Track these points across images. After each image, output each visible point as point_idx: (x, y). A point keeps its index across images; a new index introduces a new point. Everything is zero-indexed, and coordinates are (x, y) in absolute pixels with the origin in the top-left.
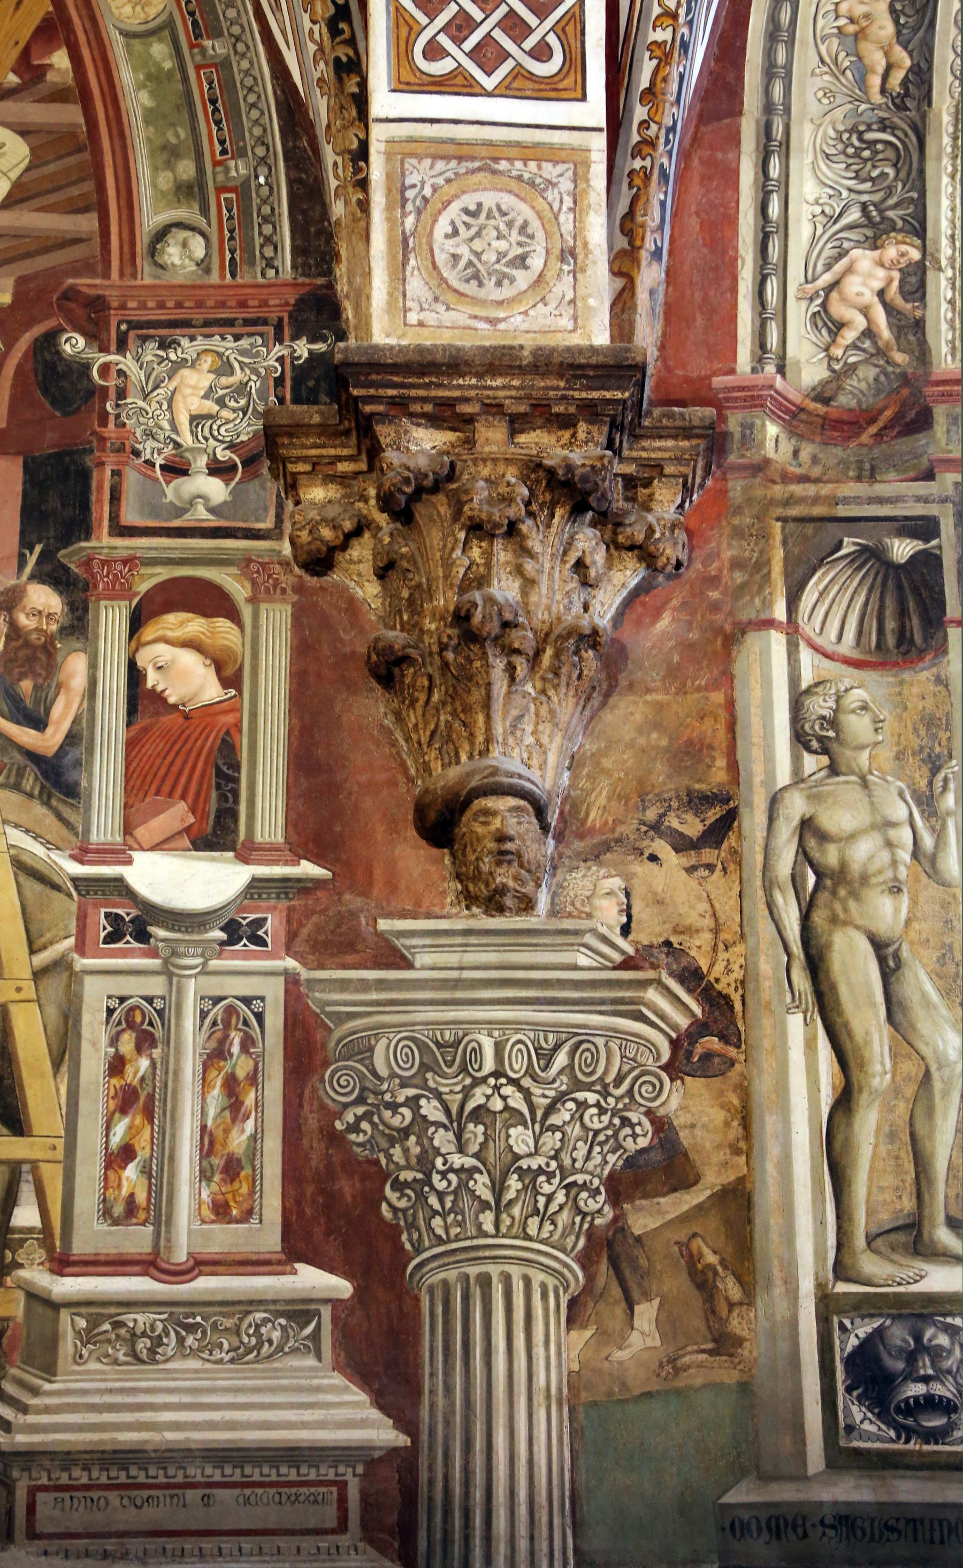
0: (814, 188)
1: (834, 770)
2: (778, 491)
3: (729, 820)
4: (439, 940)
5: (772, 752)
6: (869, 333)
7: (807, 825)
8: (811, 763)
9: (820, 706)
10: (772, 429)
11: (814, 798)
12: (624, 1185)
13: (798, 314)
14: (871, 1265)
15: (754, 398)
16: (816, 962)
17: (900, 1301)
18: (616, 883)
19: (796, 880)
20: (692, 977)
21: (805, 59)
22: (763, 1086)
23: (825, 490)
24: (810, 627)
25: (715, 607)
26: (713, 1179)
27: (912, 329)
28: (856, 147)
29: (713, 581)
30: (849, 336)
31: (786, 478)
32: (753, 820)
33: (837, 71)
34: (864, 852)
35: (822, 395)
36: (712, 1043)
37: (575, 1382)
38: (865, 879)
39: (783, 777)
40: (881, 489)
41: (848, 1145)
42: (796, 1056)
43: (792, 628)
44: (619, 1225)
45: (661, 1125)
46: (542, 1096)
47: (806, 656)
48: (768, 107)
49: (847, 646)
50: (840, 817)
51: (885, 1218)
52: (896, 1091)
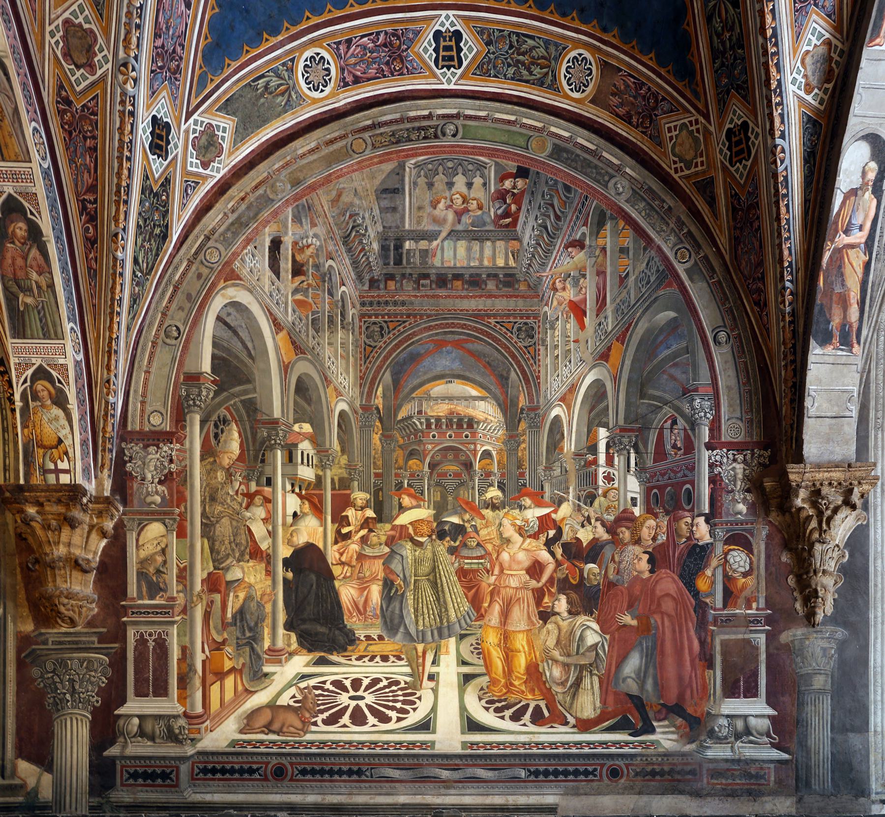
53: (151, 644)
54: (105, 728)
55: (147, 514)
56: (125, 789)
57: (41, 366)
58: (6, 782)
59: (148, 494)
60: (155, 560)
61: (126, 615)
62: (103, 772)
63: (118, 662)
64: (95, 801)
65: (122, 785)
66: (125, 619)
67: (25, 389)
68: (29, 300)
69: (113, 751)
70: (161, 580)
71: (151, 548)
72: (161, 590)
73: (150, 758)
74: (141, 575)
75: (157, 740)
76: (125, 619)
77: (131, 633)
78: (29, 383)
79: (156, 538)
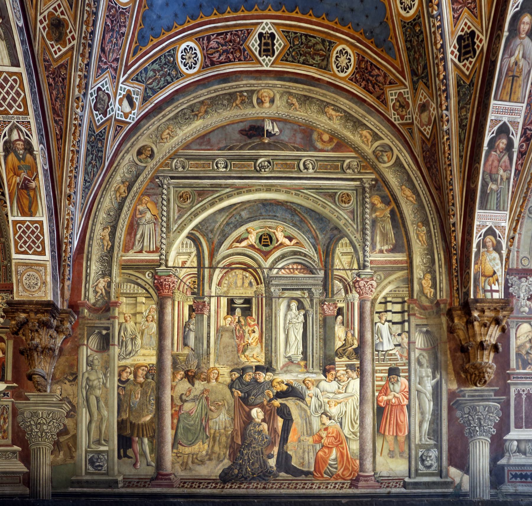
0: (95, 267)
1: (92, 369)
2: (86, 321)
3: (76, 378)
4: (33, 397)
5: (84, 367)
6: (102, 294)
7: (88, 379)
8: (89, 368)
9: (91, 359)
10: (86, 311)
11: (89, 374)
12: (59, 434)
13: (91, 290)
14: (93, 446)
15: (84, 305)
16: (88, 401)
17: (97, 451)
18: (60, 387)
19: (86, 387)
20: (70, 403)
21: (95, 243)
22: (79, 419)
23: (93, 321)
24: (90, 345)
25: (76, 341)
26: (72, 433)
27: (108, 293)
28: (102, 260)
29: (76, 337)
30: (99, 294)
31: (88, 319)
32: (80, 377)
33: (99, 246)
34: (96, 382)
35: (94, 305)
36: (72, 413)
37: (52, 463)
38: (95, 387)
39: (85, 371)
40: (102, 322)
41: (91, 429)
42: (84, 415)
43: (87, 346)
44: (58, 440)
45: (65, 425)
46: (48, 421)
47: (89, 350)
48: (88, 252)
49: (95, 349)
50: (92, 377)
51: (95, 439)
52: (98, 420)
53: (524, 397)
54: (498, 448)
55: (521, 318)
56: (510, 484)
57: (491, 227)
58: (443, 480)
59: (522, 306)
60: (526, 346)
61: (509, 379)
62: (497, 475)
63: (506, 406)
64: (493, 492)
65: (509, 482)
66: (509, 381)
67: (480, 241)
68: (494, 187)
69: (503, 461)
70: (529, 358)
71: (523, 338)
72: (529, 364)
73: (524, 465)
74: (518, 355)
75: (528, 455)
76: (509, 381)
77: (513, 390)
78: (482, 237)
79: (526, 333)
